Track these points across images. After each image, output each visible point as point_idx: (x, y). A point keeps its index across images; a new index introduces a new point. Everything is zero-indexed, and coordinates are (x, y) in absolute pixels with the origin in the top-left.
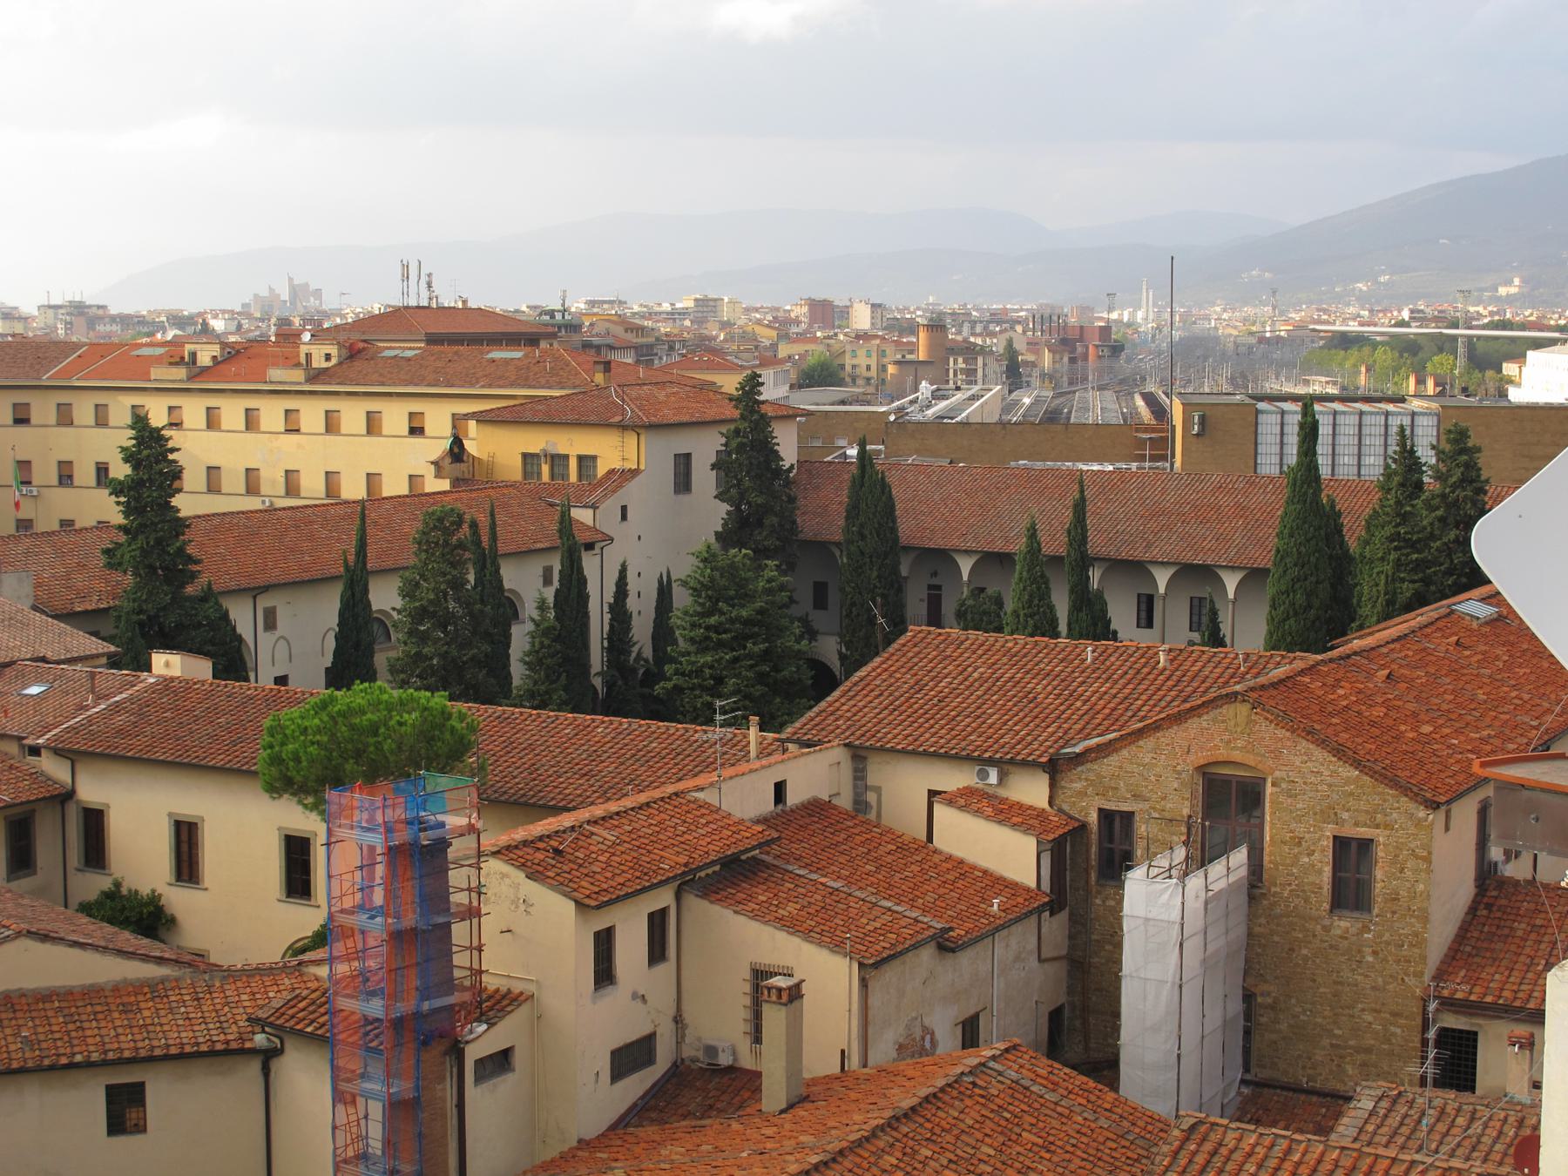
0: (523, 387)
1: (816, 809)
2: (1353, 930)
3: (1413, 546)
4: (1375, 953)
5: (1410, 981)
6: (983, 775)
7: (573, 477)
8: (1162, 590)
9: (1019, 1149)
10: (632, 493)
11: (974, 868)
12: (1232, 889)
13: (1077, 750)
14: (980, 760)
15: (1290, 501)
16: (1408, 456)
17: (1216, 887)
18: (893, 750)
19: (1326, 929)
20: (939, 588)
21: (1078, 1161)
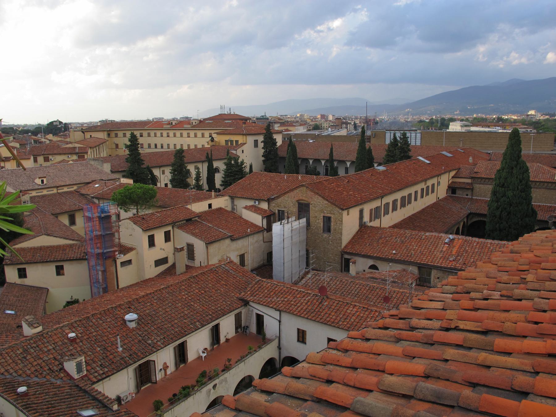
0: (229, 127)
1: (220, 210)
2: (327, 237)
3: (392, 157)
4: (332, 241)
5: (339, 248)
6: (255, 202)
7: (234, 145)
8: (348, 166)
9: (219, 285)
10: (244, 148)
11: (250, 222)
12: (300, 228)
13: (273, 197)
14: (254, 199)
15: (359, 147)
16: (395, 138)
17: (294, 228)
18: (238, 197)
19: (322, 236)
20: (307, 166)
21: (232, 288)
